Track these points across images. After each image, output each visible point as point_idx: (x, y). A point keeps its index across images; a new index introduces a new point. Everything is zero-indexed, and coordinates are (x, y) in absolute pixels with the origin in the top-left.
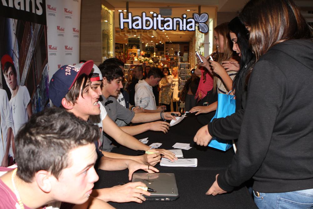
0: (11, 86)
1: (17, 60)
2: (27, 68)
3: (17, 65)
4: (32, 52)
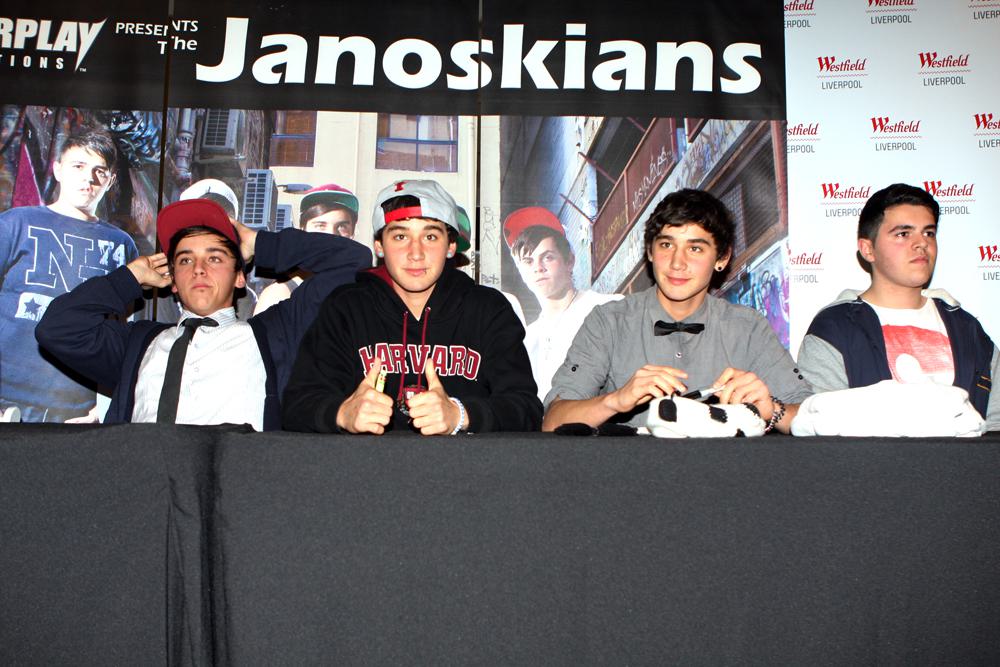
1: (586, 224)
3: (579, 232)
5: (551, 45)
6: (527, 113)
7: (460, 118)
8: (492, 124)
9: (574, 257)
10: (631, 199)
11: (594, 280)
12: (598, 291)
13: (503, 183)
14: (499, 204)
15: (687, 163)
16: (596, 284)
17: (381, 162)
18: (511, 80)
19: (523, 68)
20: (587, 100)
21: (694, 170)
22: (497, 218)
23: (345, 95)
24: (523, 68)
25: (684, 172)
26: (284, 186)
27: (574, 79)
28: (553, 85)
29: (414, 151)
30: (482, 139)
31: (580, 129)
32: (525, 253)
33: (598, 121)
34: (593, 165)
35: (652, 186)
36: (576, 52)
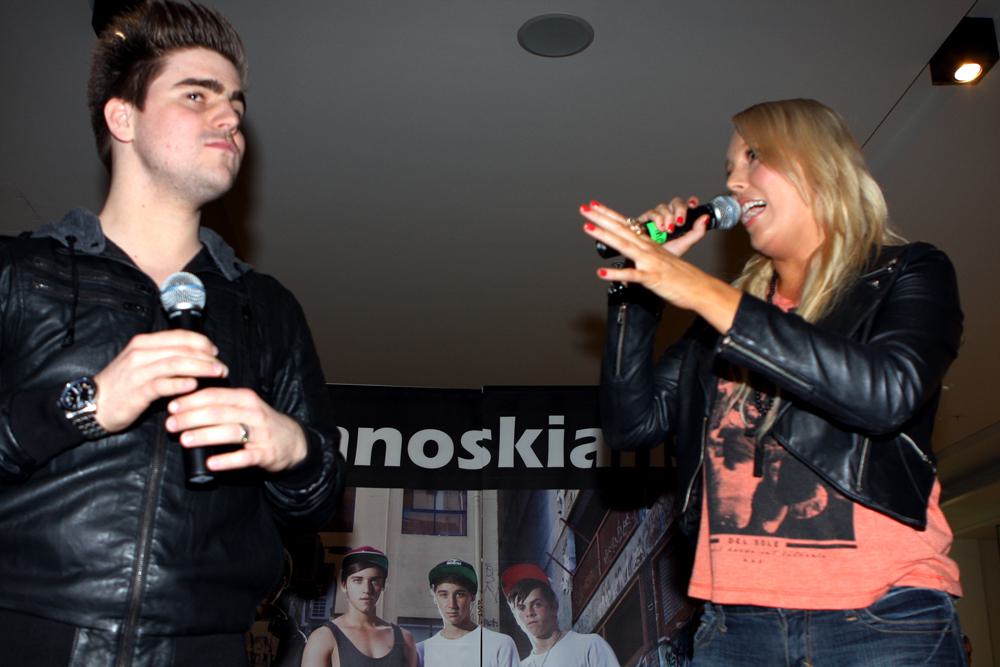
0: (533, 629)
1: (567, 576)
2: (613, 593)
3: (562, 583)
4: (640, 558)
5: (538, 432)
6: (519, 489)
7: (469, 492)
8: (492, 495)
9: (557, 604)
10: (602, 555)
11: (574, 621)
12: (578, 632)
13: (500, 543)
14: (497, 561)
15: (646, 525)
16: (577, 626)
17: (407, 528)
18: (506, 461)
19: (515, 450)
20: (567, 476)
21: (652, 531)
22: (496, 574)
23: (377, 475)
24: (515, 450)
25: (644, 533)
26: (329, 548)
27: (556, 460)
28: (538, 464)
29: (432, 520)
30: (483, 508)
31: (561, 500)
32: (519, 601)
33: (575, 493)
34: (571, 528)
35: (619, 545)
36: (556, 438)
